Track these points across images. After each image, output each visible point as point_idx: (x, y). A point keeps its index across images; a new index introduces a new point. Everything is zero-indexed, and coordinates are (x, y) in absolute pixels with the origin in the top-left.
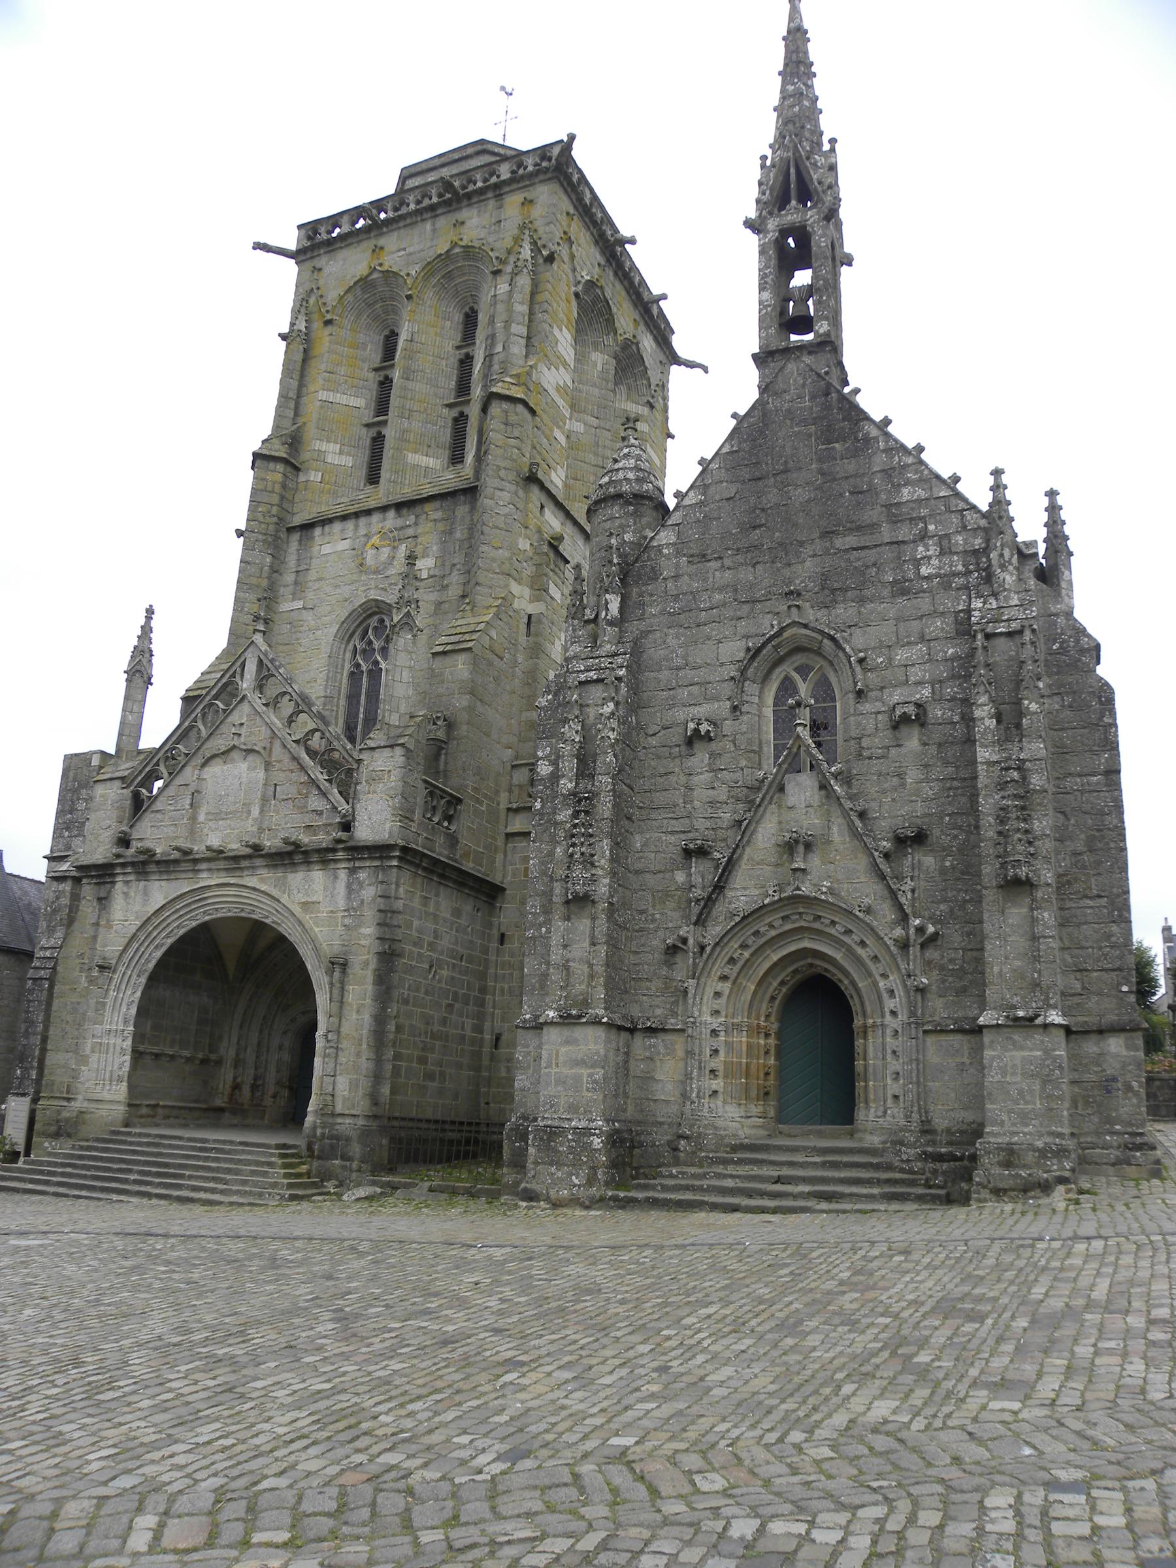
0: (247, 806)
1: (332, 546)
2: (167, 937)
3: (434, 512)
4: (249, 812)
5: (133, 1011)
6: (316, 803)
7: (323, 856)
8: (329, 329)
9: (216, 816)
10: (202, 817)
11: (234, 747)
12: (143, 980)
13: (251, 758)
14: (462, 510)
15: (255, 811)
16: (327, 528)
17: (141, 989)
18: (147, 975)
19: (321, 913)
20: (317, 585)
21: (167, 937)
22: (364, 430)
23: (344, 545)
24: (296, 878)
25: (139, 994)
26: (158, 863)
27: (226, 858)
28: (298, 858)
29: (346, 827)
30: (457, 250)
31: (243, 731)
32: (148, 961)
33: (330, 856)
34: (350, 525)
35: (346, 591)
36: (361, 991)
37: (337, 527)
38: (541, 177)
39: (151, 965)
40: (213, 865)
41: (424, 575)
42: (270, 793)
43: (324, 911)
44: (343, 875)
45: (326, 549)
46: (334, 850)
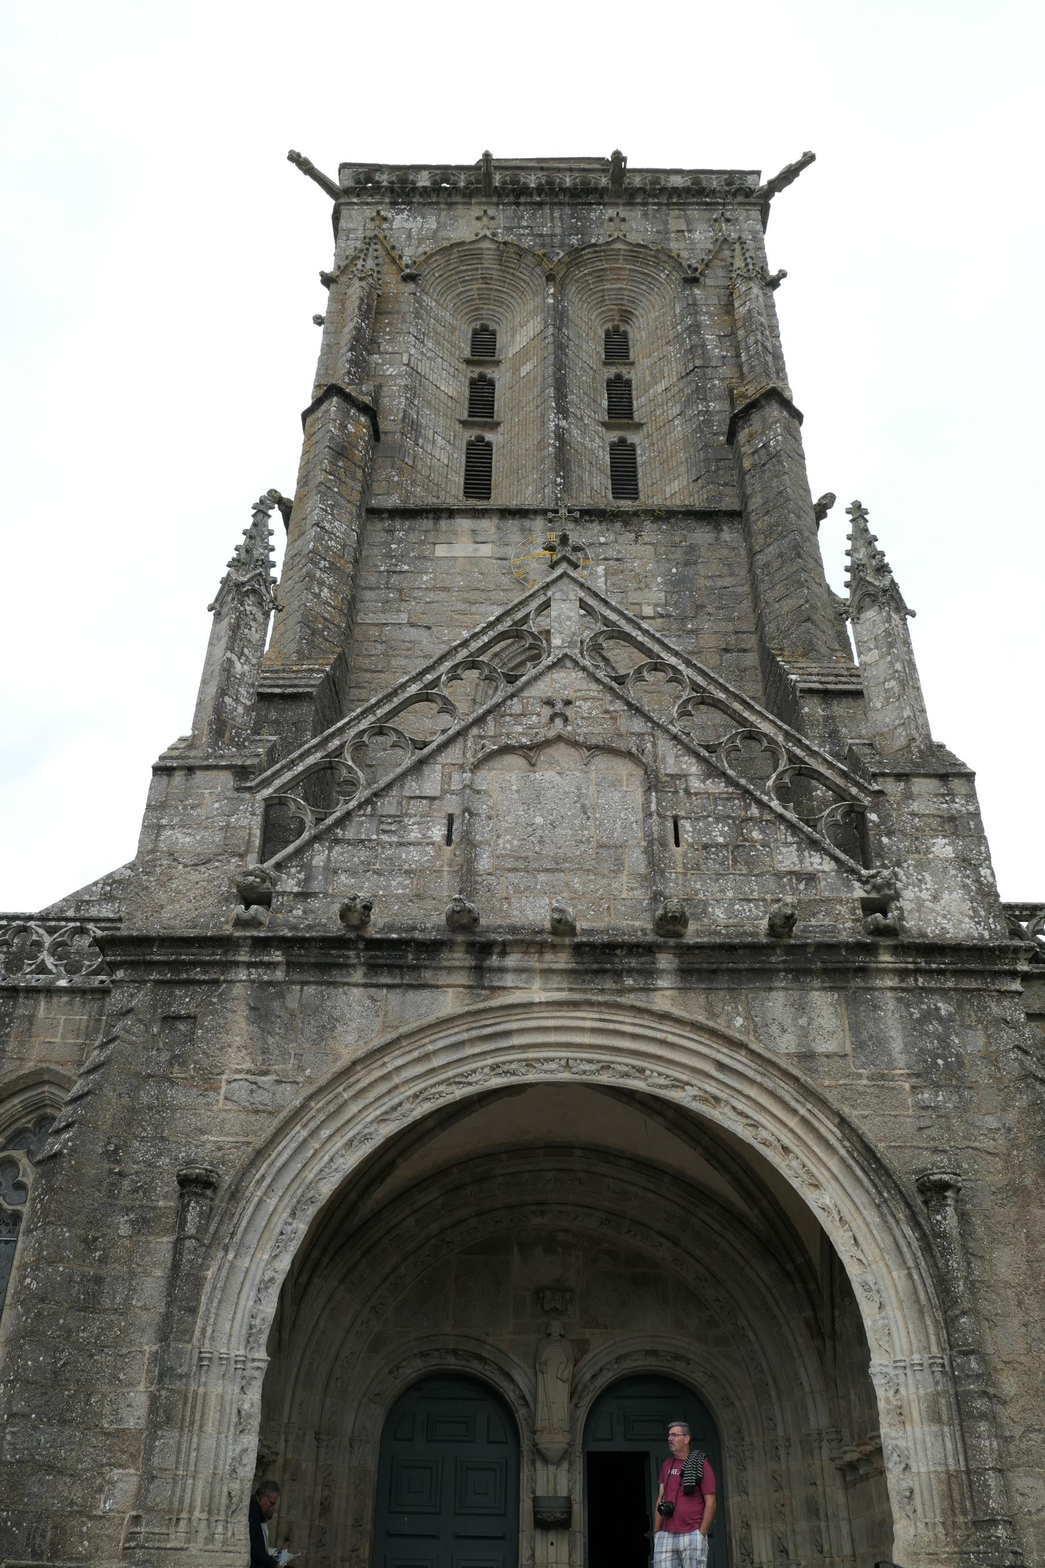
2: (381, 1120)
4: (619, 862)
5: (269, 1308)
6: (788, 857)
7: (839, 966)
8: (411, 287)
10: (484, 863)
11: (559, 738)
12: (302, 1227)
13: (602, 762)
15: (636, 859)
16: (444, 524)
17: (293, 1247)
18: (312, 1211)
20: (431, 596)
21: (381, 1120)
22: (458, 427)
23: (486, 550)
24: (777, 1003)
25: (284, 1264)
26: (373, 944)
27: (578, 949)
28: (777, 958)
30: (618, 246)
31: (569, 712)
32: (320, 1176)
33: (860, 959)
37: (464, 524)
38: (740, 199)
39: (327, 1189)
40: (533, 962)
41: (648, 611)
44: (889, 1002)
45: (441, 551)
46: (870, 949)
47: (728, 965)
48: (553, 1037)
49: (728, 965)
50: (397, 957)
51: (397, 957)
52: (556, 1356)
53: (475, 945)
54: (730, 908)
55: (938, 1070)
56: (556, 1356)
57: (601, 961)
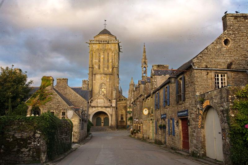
0: (102, 103)
1: (98, 77)
3: (108, 75)
6: (108, 103)
9: (99, 103)
14: (111, 76)
15: (103, 103)
19: (108, 111)
24: (107, 109)
29: (111, 105)
34: (100, 75)
35: (100, 81)
36: (114, 117)
42: (104, 102)
43: (110, 111)
47: (106, 107)
48: (100, 110)
49: (106, 107)
50: (95, 107)
51: (95, 107)
52: (103, 117)
53: (98, 107)
54: (106, 105)
55: (112, 111)
56: (103, 117)
57: (102, 107)
